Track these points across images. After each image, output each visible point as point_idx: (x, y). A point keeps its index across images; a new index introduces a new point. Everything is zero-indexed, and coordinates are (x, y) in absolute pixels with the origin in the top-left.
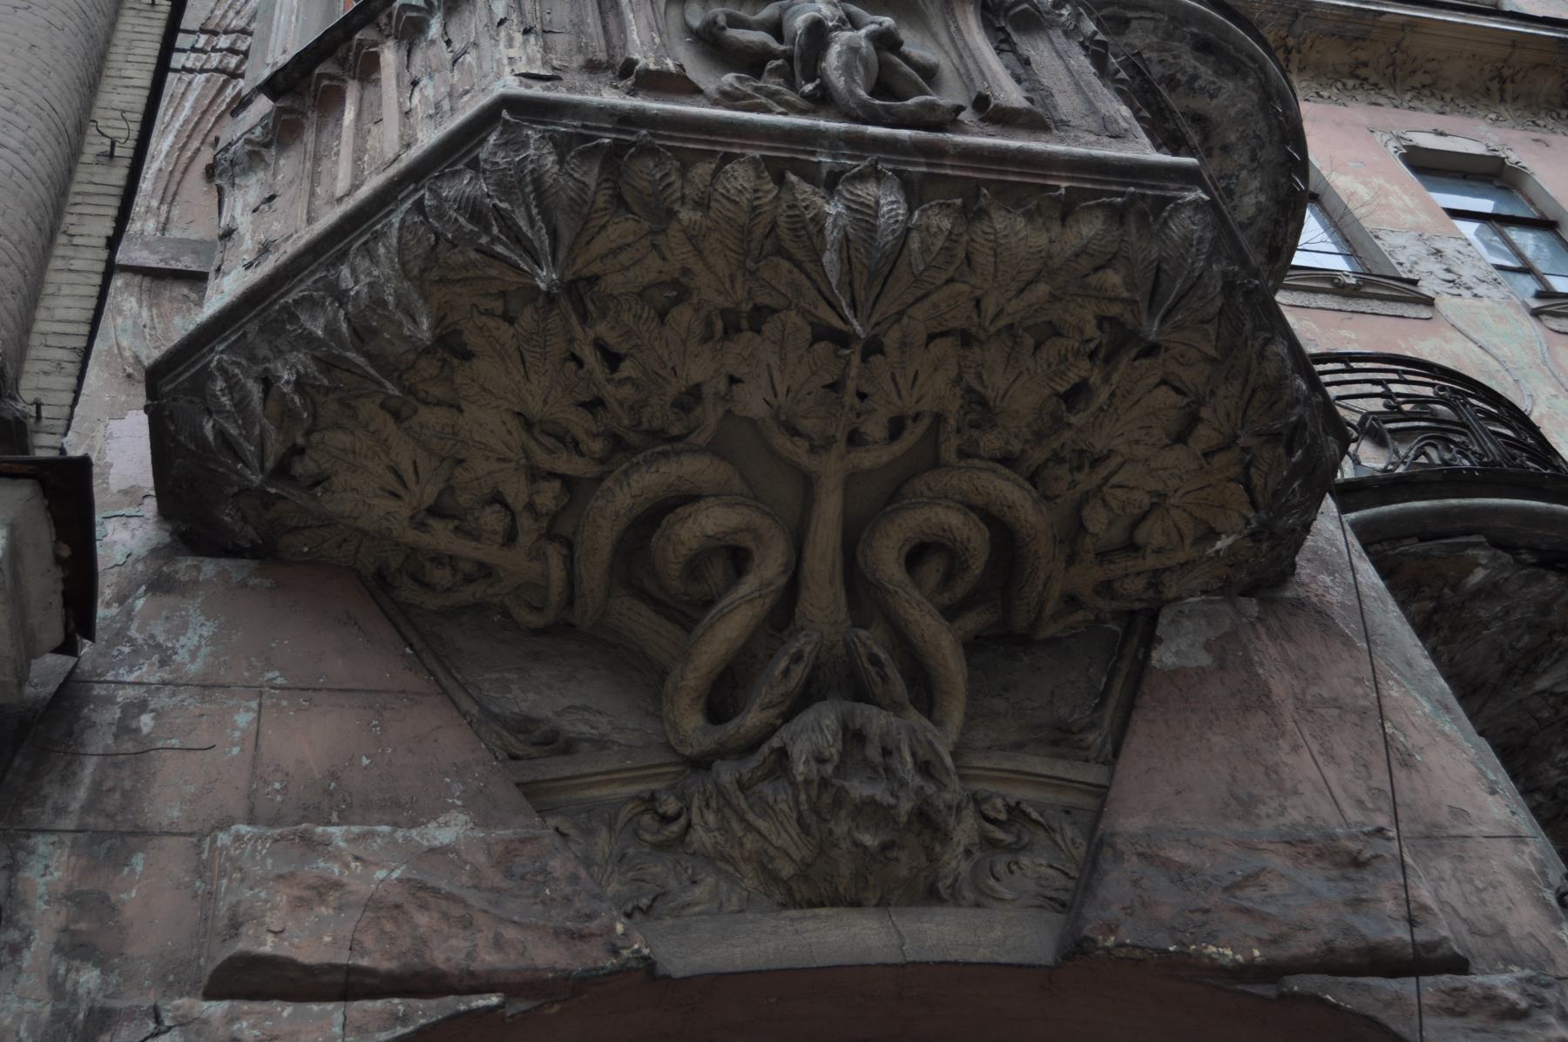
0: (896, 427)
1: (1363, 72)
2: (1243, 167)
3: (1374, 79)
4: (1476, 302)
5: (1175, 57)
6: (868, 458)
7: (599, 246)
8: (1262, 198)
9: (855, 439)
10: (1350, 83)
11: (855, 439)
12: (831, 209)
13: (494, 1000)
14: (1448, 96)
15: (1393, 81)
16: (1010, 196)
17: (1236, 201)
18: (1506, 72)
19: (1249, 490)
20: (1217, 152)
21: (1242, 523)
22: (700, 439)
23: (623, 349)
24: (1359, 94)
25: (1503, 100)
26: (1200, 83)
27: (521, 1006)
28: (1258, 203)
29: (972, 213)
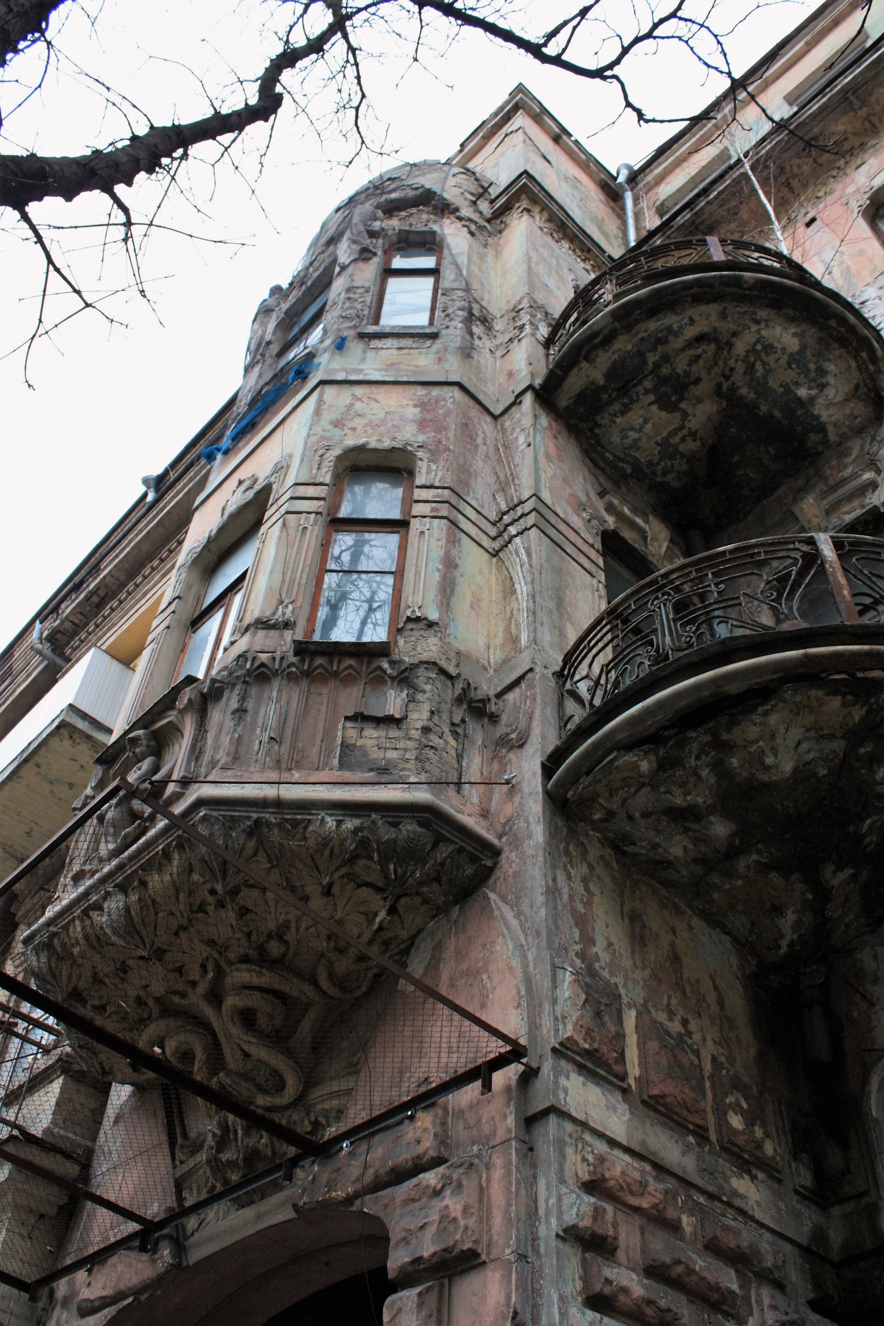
0: (203, 967)
2: (758, 331)
5: (645, 331)
6: (202, 988)
7: (64, 979)
8: (793, 330)
9: (194, 984)
11: (194, 984)
12: (104, 919)
13: (130, 1299)
16: (146, 868)
17: (779, 346)
19: (368, 885)
20: (733, 340)
21: (382, 902)
22: (156, 1013)
23: (104, 1002)
26: (675, 327)
27: (144, 1297)
29: (143, 884)
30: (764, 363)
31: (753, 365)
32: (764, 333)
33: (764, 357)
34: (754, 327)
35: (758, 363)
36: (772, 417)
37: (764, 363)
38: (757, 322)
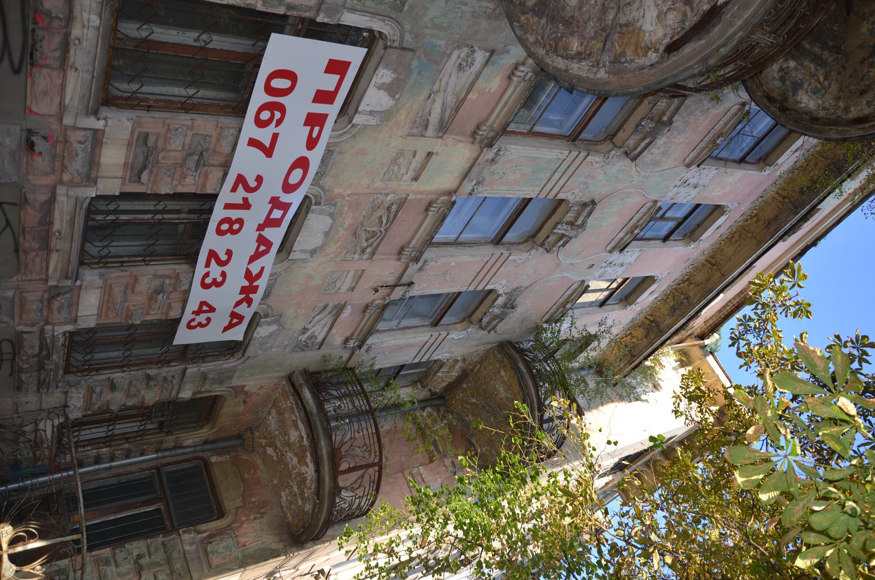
1: (755, 219)
2: (823, 103)
3: (749, 221)
4: (674, 185)
8: (802, 105)
10: (755, 212)
14: (723, 243)
15: (743, 227)
18: (715, 267)
24: (749, 212)
25: (707, 260)
28: (801, 103)
30: (818, 81)
31: (826, 78)
32: (820, 102)
33: (818, 85)
34: (827, 105)
35: (822, 80)
36: (810, 44)
37: (818, 81)
38: (824, 109)
